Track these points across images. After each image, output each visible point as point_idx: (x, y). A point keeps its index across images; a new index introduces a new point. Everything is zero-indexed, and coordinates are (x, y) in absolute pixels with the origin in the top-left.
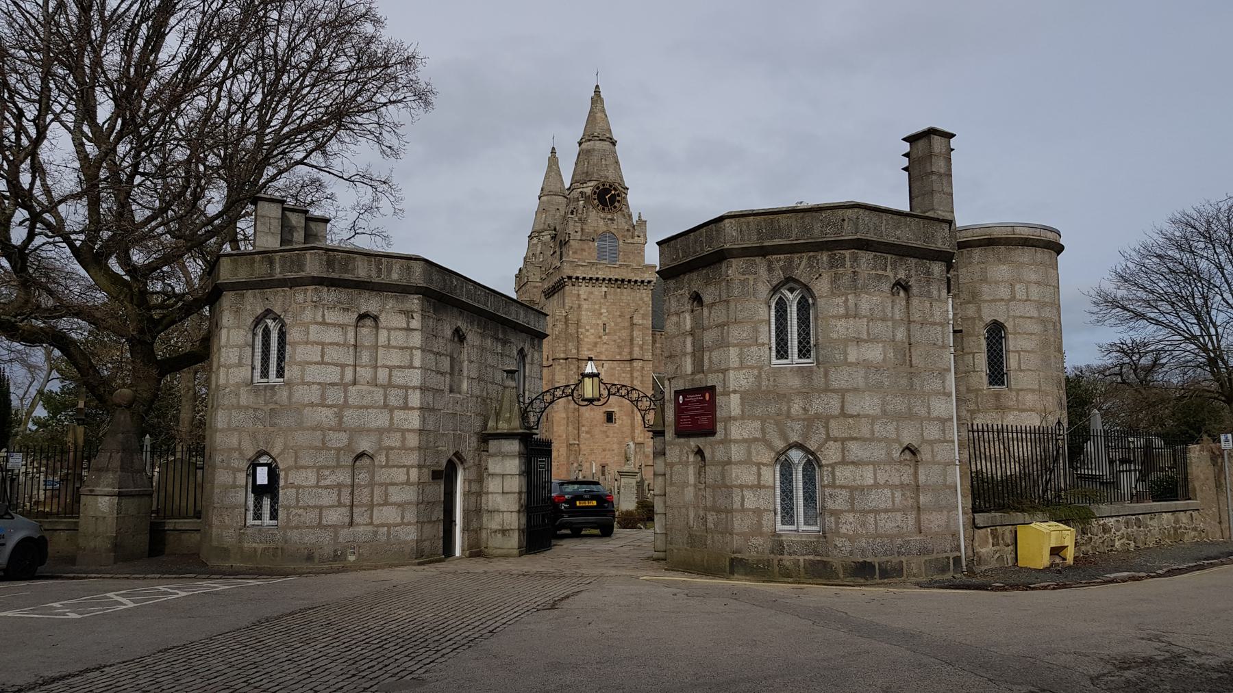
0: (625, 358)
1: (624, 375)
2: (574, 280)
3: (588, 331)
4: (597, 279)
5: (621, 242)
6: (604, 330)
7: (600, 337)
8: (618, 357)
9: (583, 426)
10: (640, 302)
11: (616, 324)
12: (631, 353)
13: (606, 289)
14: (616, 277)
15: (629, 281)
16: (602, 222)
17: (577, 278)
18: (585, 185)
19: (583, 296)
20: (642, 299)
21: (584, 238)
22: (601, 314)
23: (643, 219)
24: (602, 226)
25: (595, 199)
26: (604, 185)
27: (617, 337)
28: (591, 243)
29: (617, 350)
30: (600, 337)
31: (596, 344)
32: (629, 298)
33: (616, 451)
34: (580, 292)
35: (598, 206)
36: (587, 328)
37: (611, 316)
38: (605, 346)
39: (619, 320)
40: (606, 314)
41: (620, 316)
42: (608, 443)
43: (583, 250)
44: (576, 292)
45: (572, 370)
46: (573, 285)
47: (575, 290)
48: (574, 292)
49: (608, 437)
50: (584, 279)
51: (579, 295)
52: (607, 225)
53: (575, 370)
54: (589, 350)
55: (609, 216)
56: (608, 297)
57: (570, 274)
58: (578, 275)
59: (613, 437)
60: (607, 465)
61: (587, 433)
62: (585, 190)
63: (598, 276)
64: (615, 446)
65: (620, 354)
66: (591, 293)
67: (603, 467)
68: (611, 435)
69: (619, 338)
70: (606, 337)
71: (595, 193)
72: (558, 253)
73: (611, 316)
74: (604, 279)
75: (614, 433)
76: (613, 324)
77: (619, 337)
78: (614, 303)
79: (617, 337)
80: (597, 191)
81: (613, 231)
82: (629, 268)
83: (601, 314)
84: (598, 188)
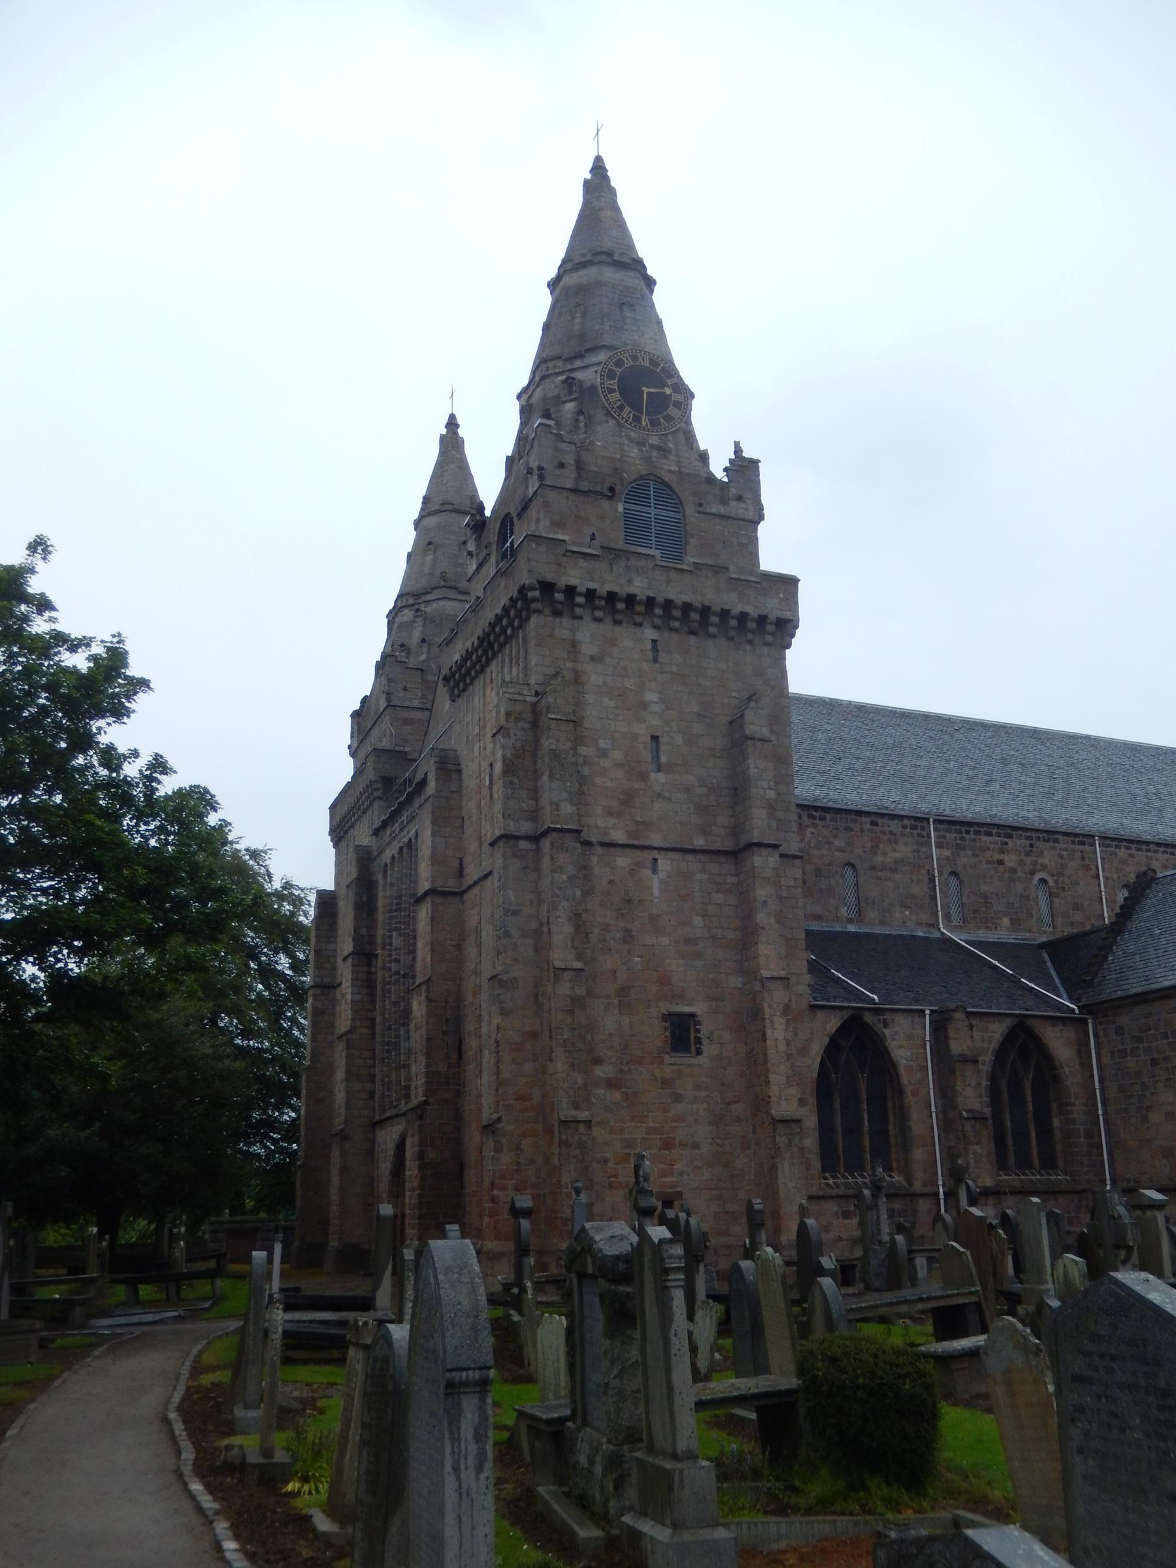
0: (718, 846)
1: (719, 898)
2: (559, 596)
3: (604, 753)
4: (631, 600)
5: (690, 510)
7: (643, 777)
8: (699, 842)
9: (597, 1061)
12: (735, 830)
14: (687, 598)
17: (570, 591)
18: (578, 363)
19: (588, 648)
21: (584, 486)
23: (747, 454)
25: (611, 391)
28: (605, 504)
31: (628, 799)
34: (580, 636)
35: (621, 408)
36: (602, 744)
38: (658, 805)
40: (657, 708)
42: (681, 1118)
44: (566, 634)
45: (561, 870)
46: (557, 614)
47: (563, 628)
48: (557, 632)
49: (678, 1099)
50: (591, 594)
51: (574, 646)
53: (571, 870)
54: (610, 813)
55: (654, 440)
56: (662, 655)
57: (550, 577)
58: (574, 582)
60: (679, 1195)
61: (612, 1084)
62: (579, 375)
63: (632, 590)
64: (702, 1132)
65: (704, 831)
70: (661, 777)
71: (611, 375)
76: (679, 739)
80: (619, 371)
81: (667, 478)
83: (644, 706)
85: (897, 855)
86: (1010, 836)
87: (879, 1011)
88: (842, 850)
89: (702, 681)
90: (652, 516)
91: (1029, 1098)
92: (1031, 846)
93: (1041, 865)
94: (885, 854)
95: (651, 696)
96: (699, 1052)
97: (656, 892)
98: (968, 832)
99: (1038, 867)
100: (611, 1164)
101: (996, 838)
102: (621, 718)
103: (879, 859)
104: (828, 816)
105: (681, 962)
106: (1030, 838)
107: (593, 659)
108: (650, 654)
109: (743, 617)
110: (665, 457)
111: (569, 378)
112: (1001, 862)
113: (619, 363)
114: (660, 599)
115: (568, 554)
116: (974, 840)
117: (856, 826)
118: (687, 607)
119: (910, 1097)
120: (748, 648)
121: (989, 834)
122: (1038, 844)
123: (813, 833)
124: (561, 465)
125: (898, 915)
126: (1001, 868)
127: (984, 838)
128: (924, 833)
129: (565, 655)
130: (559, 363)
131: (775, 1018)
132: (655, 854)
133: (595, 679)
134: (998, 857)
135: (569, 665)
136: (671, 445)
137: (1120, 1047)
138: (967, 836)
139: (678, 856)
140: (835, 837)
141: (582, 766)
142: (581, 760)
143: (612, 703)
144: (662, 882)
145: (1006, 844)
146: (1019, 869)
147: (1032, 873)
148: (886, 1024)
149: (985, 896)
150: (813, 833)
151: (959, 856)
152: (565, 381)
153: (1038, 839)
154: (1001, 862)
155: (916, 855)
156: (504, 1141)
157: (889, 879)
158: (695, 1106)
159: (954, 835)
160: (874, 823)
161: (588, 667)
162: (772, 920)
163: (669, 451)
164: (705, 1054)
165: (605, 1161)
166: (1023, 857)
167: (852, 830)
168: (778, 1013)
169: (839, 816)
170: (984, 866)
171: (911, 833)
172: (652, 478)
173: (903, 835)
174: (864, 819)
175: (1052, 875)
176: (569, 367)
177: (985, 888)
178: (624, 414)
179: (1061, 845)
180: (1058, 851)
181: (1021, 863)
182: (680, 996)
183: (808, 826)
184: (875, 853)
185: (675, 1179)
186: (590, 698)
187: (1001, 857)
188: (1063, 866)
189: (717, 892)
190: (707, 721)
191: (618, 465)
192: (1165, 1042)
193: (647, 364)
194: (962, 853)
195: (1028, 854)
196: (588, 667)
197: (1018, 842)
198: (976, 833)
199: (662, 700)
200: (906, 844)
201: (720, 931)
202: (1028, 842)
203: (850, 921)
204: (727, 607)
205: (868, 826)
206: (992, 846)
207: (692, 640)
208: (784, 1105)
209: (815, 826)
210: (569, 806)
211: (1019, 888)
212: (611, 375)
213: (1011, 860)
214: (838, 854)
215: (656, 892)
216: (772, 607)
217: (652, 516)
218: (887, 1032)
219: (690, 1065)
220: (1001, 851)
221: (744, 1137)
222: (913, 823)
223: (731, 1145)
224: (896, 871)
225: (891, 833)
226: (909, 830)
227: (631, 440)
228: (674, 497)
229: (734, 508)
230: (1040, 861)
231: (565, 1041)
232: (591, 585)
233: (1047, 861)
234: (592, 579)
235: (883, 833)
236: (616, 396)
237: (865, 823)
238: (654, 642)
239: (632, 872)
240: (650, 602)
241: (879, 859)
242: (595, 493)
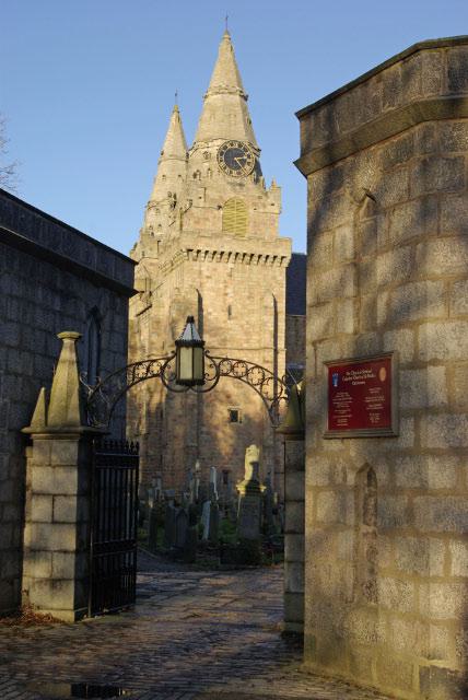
0: (253, 346)
6: (230, 314)
8: (245, 346)
9: (203, 425)
11: (244, 307)
17: (199, 251)
18: (210, 144)
19: (206, 273)
20: (274, 278)
24: (230, 194)
27: (244, 322)
28: (216, 212)
41: (249, 298)
43: (207, 219)
44: (196, 268)
48: (195, 268)
51: (200, 272)
66: (215, 270)
69: (248, 323)
71: (222, 154)
72: (178, 223)
73: (237, 297)
76: (239, 306)
83: (226, 294)
84: (225, 148)
95: (229, 291)
107: (208, 277)
135: (198, 280)
186: (205, 292)
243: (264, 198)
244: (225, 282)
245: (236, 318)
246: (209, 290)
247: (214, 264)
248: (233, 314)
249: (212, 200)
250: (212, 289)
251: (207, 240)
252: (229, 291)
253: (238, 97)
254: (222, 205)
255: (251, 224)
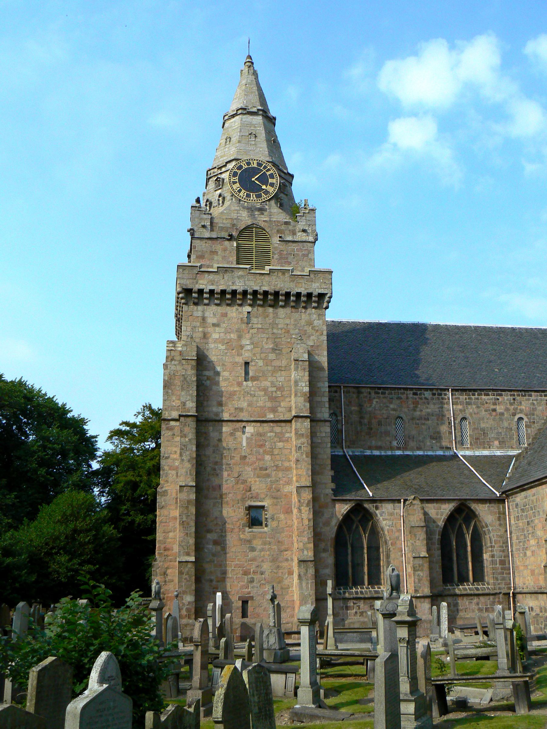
4: (234, 293)
5: (275, 240)
6: (247, 373)
8: (271, 416)
9: (209, 531)
10: (309, 330)
11: (268, 363)
13: (249, 309)
14: (266, 288)
15: (288, 295)
16: (244, 214)
17: (201, 292)
18: (224, 169)
19: (211, 320)
20: (310, 323)
21: (214, 235)
22: (242, 347)
24: (245, 219)
25: (234, 183)
26: (248, 164)
27: (268, 384)
28: (227, 243)
29: (269, 404)
30: (240, 384)
32: (288, 321)
33: (266, 575)
34: (207, 314)
35: (240, 191)
37: (258, 350)
38: (249, 398)
39: (272, 356)
40: (249, 347)
41: (274, 350)
42: (253, 559)
43: (214, 253)
45: (185, 436)
48: (195, 314)
49: (253, 549)
50: (212, 292)
51: (204, 319)
52: (252, 216)
56: (254, 320)
57: (190, 287)
58: (201, 287)
59: (262, 550)
60: (252, 598)
61: (216, 543)
62: (223, 176)
63: (234, 288)
65: (274, 410)
66: (225, 315)
67: (245, 603)
68: (259, 547)
69: (273, 384)
71: (235, 174)
73: (258, 350)
74: (245, 293)
75: (264, 543)
76: (261, 363)
77: (272, 383)
78: (262, 330)
79: (269, 384)
81: (262, 225)
82: (287, 275)
83: (242, 347)
84: (240, 167)
85: (429, 410)
86: (501, 395)
87: (373, 501)
88: (394, 410)
89: (275, 331)
90: (254, 246)
91: (469, 544)
92: (514, 399)
93: (520, 410)
94: (421, 411)
96: (266, 526)
97: (244, 444)
98: (474, 395)
99: (518, 411)
100: (214, 583)
101: (491, 397)
102: (228, 354)
103: (418, 413)
104: (387, 392)
105: (257, 479)
106: (514, 395)
107: (214, 325)
108: (245, 320)
109: (298, 295)
110: (263, 214)
111: (218, 178)
112: (494, 410)
113: (240, 167)
114: (250, 291)
115: (199, 273)
116: (478, 399)
117: (403, 397)
118: (266, 293)
119: (390, 546)
120: (303, 310)
121: (488, 395)
122: (518, 398)
123: (377, 402)
124: (204, 226)
125: (428, 443)
126: (494, 413)
127: (483, 397)
128: (446, 397)
129: (198, 324)
130: (216, 170)
131: (302, 508)
132: (244, 424)
133: (215, 336)
134: (493, 407)
135: (201, 329)
136: (267, 207)
137: (517, 515)
138: (473, 397)
139: (258, 424)
140: (391, 403)
141: (206, 381)
142: (205, 378)
143: (223, 347)
144: (247, 438)
145: (498, 399)
146: (505, 413)
147: (514, 415)
148: (377, 508)
149: (483, 430)
150: (377, 402)
151: (467, 408)
152: (216, 180)
153: (518, 395)
154: (494, 410)
155: (441, 410)
156: (158, 570)
157: (424, 424)
158: (262, 553)
159: (465, 397)
160: (415, 394)
161: (211, 329)
162: (304, 456)
163: (266, 210)
164: (269, 527)
165: (211, 581)
166: (508, 406)
167: (401, 398)
168: (305, 505)
169: (393, 392)
170: (483, 413)
171: (438, 398)
172: (255, 226)
173: (433, 399)
174: (409, 392)
175: (526, 415)
176: (220, 172)
177: (483, 425)
178: (241, 194)
179: (533, 397)
180: (531, 401)
181: (507, 410)
182: (256, 497)
183: (374, 398)
184: (414, 410)
185: (250, 590)
186: (212, 346)
187: (494, 407)
188: (535, 409)
189: (280, 442)
190: (277, 352)
191: (235, 222)
192: (532, 512)
193: (255, 165)
194: (469, 407)
195: (511, 404)
196: (211, 329)
197: (506, 398)
198: (478, 395)
199: (252, 343)
200: (434, 404)
201: (280, 462)
202: (512, 397)
203: (399, 449)
204: (288, 291)
205: (411, 396)
206: (488, 401)
207: (271, 310)
208: (305, 552)
209: (379, 398)
210: (191, 403)
211: (506, 424)
212: (235, 174)
213: (500, 409)
214: (392, 412)
215: (244, 444)
216: (316, 288)
217: (254, 246)
218: (377, 512)
219: (260, 533)
220: (495, 404)
221: (290, 569)
222: (439, 392)
223: (282, 573)
224: (428, 419)
225: (426, 398)
226: (437, 396)
227: (244, 208)
228: (267, 234)
229: (300, 236)
230: (519, 408)
231: (183, 522)
232: (212, 287)
233: (524, 407)
234: (213, 284)
235: (421, 399)
236: (238, 185)
237: (410, 394)
238: (249, 313)
239: (232, 434)
240: (245, 293)
241: (418, 413)
242: (221, 238)
243: (292, 223)
244: (238, 331)
245: (255, 379)
246: (216, 341)
247: (224, 309)
248: (251, 374)
249: (222, 229)
250: (222, 342)
251: (211, 276)
252: (245, 341)
253: (260, 118)
254: (235, 234)
255: (276, 256)
